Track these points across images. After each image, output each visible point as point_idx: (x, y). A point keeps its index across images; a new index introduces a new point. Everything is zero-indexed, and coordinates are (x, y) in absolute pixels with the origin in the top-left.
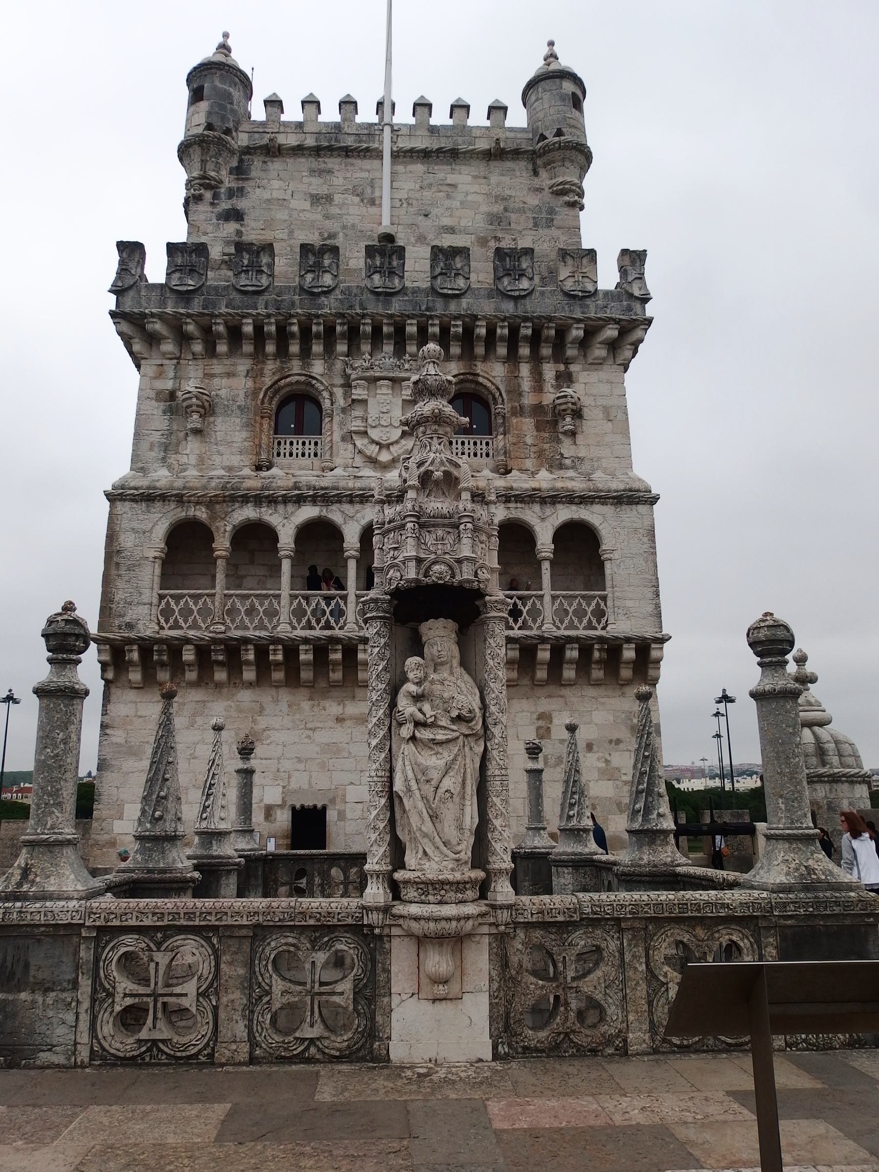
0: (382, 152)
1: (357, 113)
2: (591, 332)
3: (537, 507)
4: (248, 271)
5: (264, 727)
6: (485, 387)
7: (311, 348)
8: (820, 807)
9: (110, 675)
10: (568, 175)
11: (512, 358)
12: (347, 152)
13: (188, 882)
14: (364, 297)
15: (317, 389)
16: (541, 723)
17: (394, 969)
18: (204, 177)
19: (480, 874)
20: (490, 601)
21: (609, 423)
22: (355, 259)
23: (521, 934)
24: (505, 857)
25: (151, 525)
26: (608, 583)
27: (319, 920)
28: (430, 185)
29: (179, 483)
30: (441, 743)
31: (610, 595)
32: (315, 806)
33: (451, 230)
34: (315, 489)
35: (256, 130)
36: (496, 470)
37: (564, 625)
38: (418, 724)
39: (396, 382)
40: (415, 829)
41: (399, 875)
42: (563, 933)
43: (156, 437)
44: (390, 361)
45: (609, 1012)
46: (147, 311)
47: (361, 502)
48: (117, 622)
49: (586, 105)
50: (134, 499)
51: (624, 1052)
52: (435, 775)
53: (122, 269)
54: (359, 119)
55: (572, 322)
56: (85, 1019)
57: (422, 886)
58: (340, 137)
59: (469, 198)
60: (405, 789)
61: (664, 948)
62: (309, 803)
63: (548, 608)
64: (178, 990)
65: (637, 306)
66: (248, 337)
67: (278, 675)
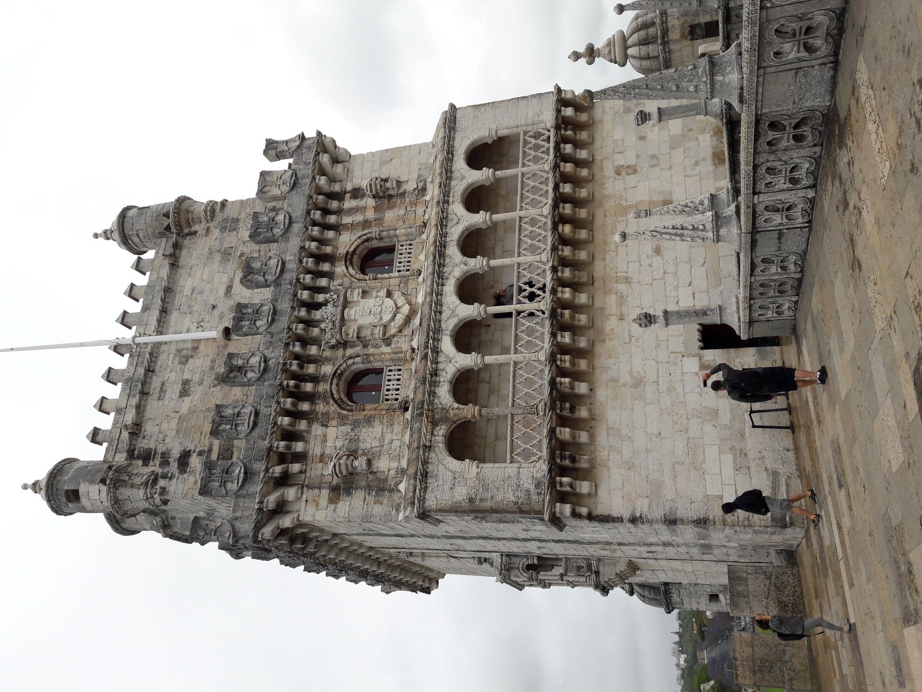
2: (323, 173)
3: (453, 183)
5: (629, 377)
6: (358, 246)
11: (336, 228)
12: (150, 371)
15: (345, 370)
16: (623, 173)
25: (449, 473)
26: (515, 131)
31: (524, 128)
32: (699, 331)
39: (346, 304)
47: (442, 305)
58: (136, 377)
59: (205, 277)
62: (697, 336)
65: (306, 143)
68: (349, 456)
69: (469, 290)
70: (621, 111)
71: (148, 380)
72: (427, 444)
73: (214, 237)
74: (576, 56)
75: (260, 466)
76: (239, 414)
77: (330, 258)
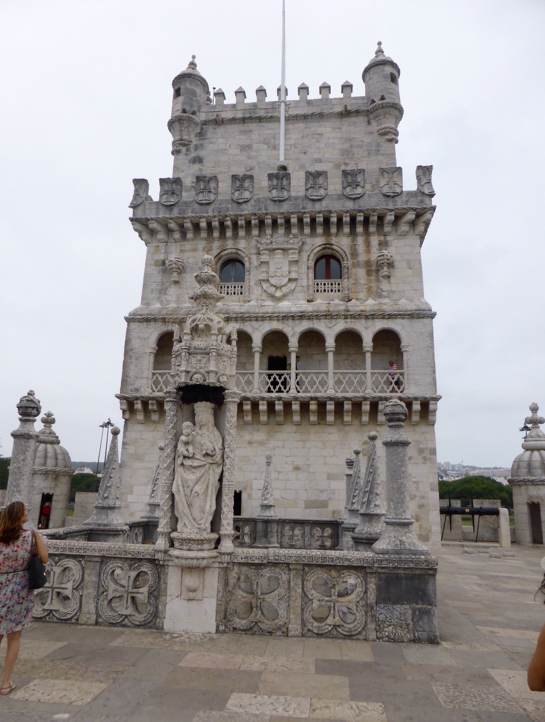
0: (279, 118)
1: (266, 96)
3: (363, 321)
4: (203, 192)
6: (337, 251)
7: (238, 234)
9: (127, 416)
10: (388, 123)
11: (353, 233)
12: (260, 119)
13: (119, 531)
14: (267, 203)
15: (242, 256)
17: (169, 582)
18: (181, 140)
19: (215, 536)
20: (228, 393)
21: (410, 270)
23: (236, 568)
24: (228, 528)
26: (405, 365)
27: (133, 555)
28: (308, 135)
29: (164, 312)
30: (195, 467)
31: (406, 372)
33: (319, 161)
34: (237, 314)
35: (210, 110)
36: (343, 300)
37: (378, 390)
38: (185, 457)
40: (180, 511)
41: (174, 535)
42: (259, 569)
43: (154, 286)
45: (280, 612)
46: (149, 217)
47: (263, 320)
48: (130, 388)
49: (400, 80)
51: (286, 634)
52: (191, 484)
53: (136, 194)
54: (267, 100)
55: (386, 211)
57: (180, 541)
58: (257, 111)
59: (330, 141)
60: (177, 490)
63: (369, 381)
64: (63, 586)
65: (427, 199)
69: (275, 339)
70: (421, 446)
71: (254, 120)
72: (166, 320)
74: (534, 409)
75: (175, 213)
76: (210, 192)
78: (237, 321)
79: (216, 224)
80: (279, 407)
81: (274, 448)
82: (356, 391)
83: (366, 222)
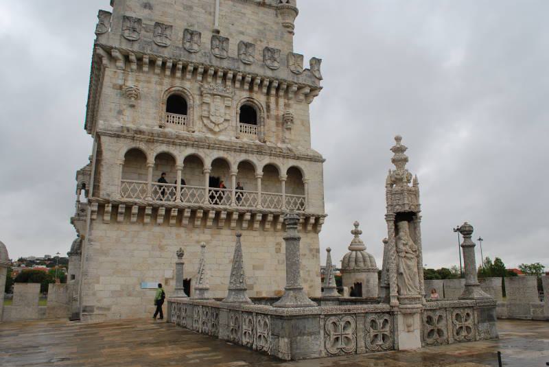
2: (299, 89)
3: (281, 159)
8: (363, 281)
15: (187, 95)
22: (206, 37)
26: (306, 192)
33: (242, 33)
38: (406, 253)
44: (221, 88)
46: (113, 46)
47: (212, 149)
50: (110, 136)
56: (323, 343)
61: (454, 314)
65: (317, 81)
66: (158, 66)
67: (173, 221)
68: (137, 95)
69: (220, 164)
73: (274, 26)
75: (136, 47)
77: (251, 90)
78: (193, 146)
79: (169, 64)
80: (223, 216)
81: (216, 246)
82: (275, 207)
83: (278, 89)
